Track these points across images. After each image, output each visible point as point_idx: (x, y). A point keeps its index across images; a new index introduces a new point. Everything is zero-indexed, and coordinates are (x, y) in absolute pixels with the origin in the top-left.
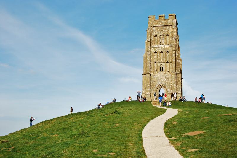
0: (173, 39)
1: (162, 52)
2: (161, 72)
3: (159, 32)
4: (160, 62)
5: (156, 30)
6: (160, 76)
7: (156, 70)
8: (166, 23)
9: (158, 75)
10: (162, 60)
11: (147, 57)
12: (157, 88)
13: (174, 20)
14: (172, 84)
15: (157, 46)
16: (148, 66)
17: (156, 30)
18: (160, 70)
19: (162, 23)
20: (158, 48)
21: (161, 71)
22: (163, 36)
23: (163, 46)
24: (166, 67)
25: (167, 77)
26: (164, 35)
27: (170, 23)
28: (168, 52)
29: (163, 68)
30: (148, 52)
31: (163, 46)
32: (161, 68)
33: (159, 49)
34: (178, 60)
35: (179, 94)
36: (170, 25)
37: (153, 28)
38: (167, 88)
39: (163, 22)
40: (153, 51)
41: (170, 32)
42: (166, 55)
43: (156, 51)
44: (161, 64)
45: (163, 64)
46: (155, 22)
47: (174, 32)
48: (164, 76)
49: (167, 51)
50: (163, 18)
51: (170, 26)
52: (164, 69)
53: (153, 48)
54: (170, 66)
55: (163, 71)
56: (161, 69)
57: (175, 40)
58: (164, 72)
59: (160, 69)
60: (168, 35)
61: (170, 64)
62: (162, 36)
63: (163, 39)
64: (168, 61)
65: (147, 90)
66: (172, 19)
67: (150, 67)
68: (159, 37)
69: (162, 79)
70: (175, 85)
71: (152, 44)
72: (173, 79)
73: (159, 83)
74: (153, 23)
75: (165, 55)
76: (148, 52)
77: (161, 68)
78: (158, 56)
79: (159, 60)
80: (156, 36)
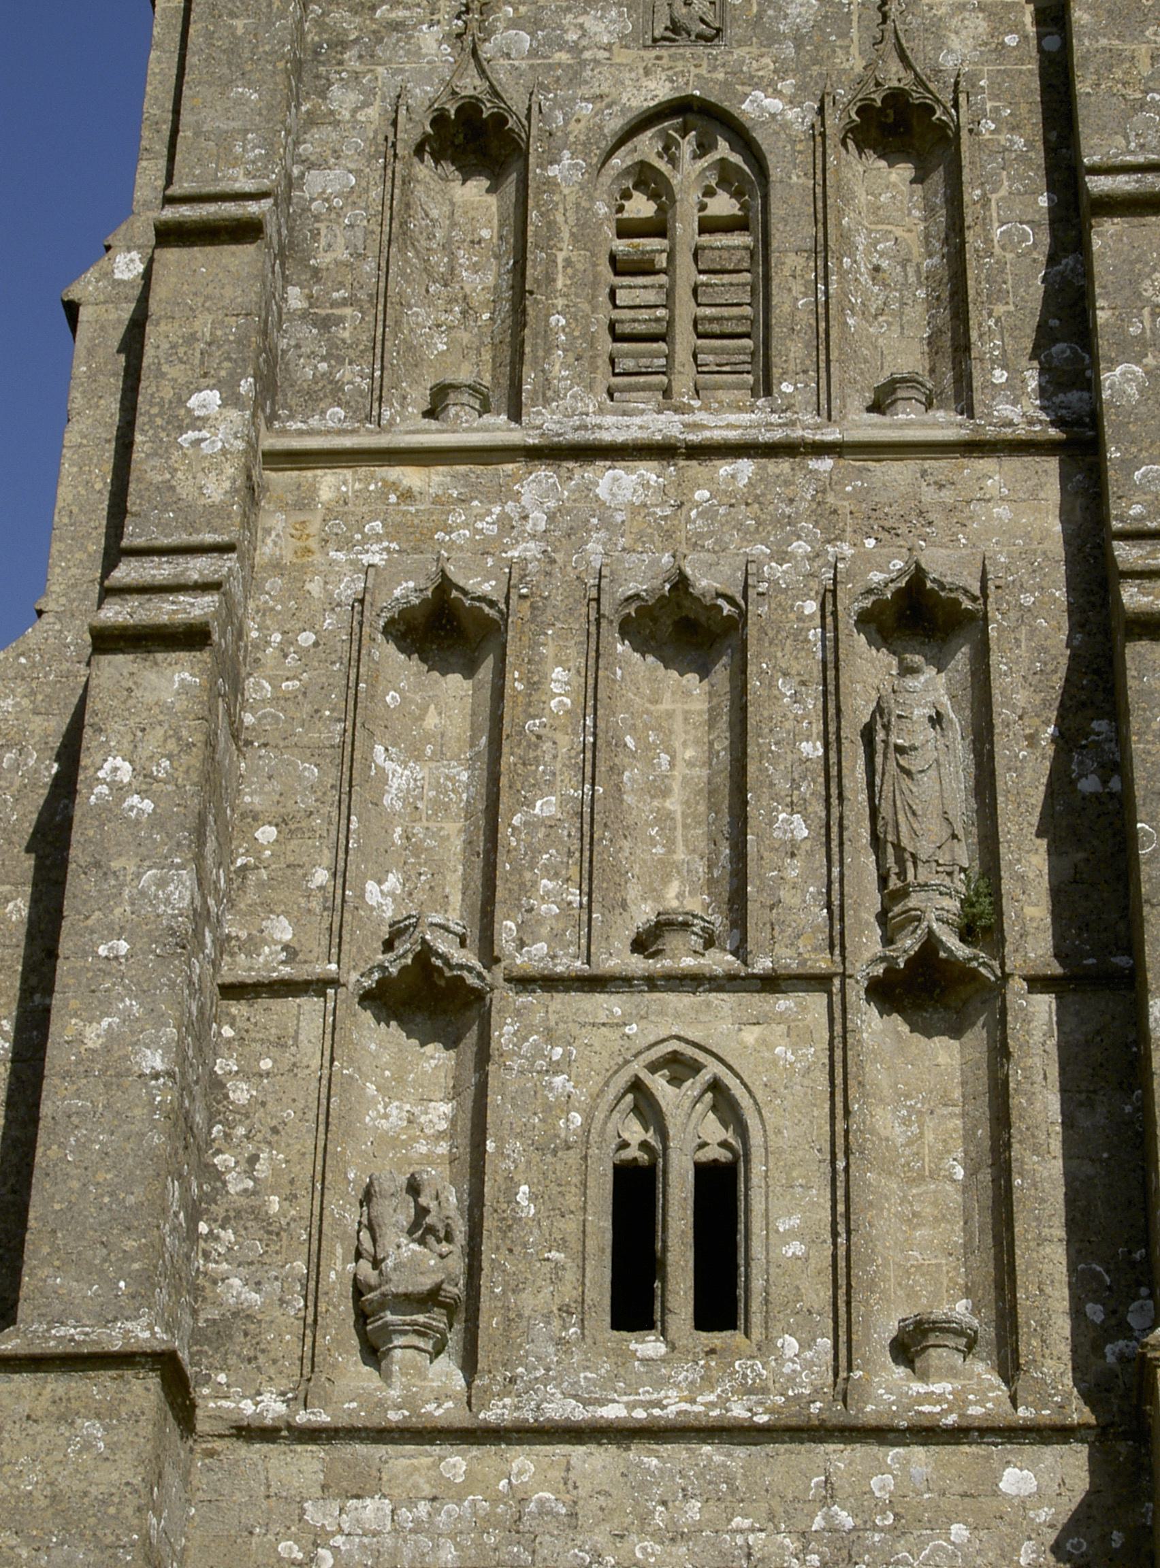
2: (668, 1372)
7: (414, 1263)
9: (523, 1462)
16: (113, 1069)
20: (537, 487)
21: (634, 1307)
22: (723, 149)
33: (568, 527)
45: (722, 1026)
49: (884, 572)
52: (784, 1232)
53: (329, 484)
55: (719, 1305)
71: (306, 371)
77: (635, 1188)
79: (551, 894)
80: (476, 139)
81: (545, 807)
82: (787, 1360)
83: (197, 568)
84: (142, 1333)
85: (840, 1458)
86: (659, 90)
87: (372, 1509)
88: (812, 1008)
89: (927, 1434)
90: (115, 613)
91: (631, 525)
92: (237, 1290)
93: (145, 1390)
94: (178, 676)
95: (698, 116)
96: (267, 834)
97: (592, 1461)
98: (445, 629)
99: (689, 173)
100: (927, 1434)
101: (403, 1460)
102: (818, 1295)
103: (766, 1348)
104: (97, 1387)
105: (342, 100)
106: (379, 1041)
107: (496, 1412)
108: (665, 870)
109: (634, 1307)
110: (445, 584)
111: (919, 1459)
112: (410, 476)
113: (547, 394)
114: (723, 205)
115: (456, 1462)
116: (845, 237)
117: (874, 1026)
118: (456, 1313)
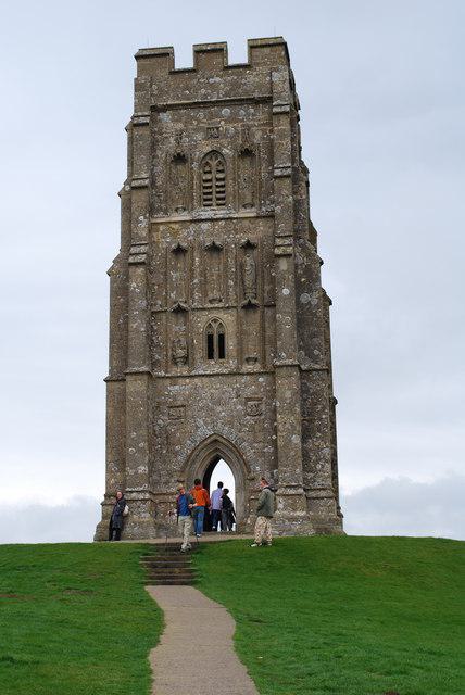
0: (278, 173)
1: (214, 249)
2: (214, 367)
3: (199, 136)
4: (210, 306)
5: (180, 126)
6: (210, 389)
7: (181, 352)
8: (235, 85)
10: (216, 294)
11: (128, 279)
12: (189, 460)
13: (277, 70)
14: (275, 431)
15: (185, 216)
17: (180, 126)
18: (205, 353)
19: (213, 86)
20: (192, 228)
21: (210, 356)
23: (221, 213)
24: (241, 334)
25: (248, 392)
26: (225, 151)
27: (259, 86)
28: (249, 246)
29: (222, 338)
30: (133, 250)
31: (221, 213)
32: (210, 338)
33: (197, 234)
34: (310, 291)
35: (322, 494)
36: (256, 95)
37: (165, 117)
38: (250, 454)
39: (218, 79)
40: (166, 242)
41: (258, 135)
42: (242, 266)
43: (184, 245)
44: (215, 314)
46: (172, 81)
47: (282, 135)
48: (228, 388)
50: (216, 60)
51: (256, 102)
52: (230, 344)
53: (161, 228)
54: (267, 325)
55: (222, 355)
56: (215, 347)
57: (288, 181)
58: (231, 364)
59: (206, 345)
60: (246, 153)
61: (263, 317)
62: (214, 163)
63: (221, 176)
64: (253, 301)
65: (131, 472)
66: (265, 64)
67: (149, 338)
68: (195, 165)
69: (218, 402)
70: (296, 439)
72: (283, 400)
73: (205, 431)
74: (160, 90)
75: (231, 262)
76: (133, 250)
77: (210, 338)
78: (192, 271)
79: (197, 295)
81: (196, 281)
82: (232, 364)
83: (143, 249)
84: (145, 368)
85: (238, 378)
86: (209, 149)
87: (177, 387)
88: (234, 312)
89: (248, 374)
90: (131, 260)
91: (207, 234)
92: (157, 357)
93: (145, 377)
94: (140, 270)
95: (214, 153)
96: (156, 287)
97: (205, 380)
98: (179, 251)
99: (214, 163)
100: (248, 374)
101: (180, 381)
102: (235, 354)
103: (228, 362)
104: (139, 377)
105: (159, 153)
106: (173, 318)
107: (193, 373)
108: (214, 288)
109: (210, 356)
110: (179, 245)
111: (248, 378)
112: (173, 226)
113: (192, 209)
114: (220, 168)
115: (187, 381)
116: (239, 177)
117: (242, 313)
118: (186, 360)
